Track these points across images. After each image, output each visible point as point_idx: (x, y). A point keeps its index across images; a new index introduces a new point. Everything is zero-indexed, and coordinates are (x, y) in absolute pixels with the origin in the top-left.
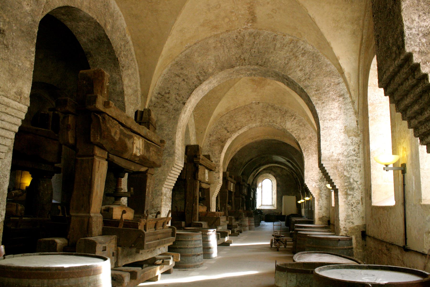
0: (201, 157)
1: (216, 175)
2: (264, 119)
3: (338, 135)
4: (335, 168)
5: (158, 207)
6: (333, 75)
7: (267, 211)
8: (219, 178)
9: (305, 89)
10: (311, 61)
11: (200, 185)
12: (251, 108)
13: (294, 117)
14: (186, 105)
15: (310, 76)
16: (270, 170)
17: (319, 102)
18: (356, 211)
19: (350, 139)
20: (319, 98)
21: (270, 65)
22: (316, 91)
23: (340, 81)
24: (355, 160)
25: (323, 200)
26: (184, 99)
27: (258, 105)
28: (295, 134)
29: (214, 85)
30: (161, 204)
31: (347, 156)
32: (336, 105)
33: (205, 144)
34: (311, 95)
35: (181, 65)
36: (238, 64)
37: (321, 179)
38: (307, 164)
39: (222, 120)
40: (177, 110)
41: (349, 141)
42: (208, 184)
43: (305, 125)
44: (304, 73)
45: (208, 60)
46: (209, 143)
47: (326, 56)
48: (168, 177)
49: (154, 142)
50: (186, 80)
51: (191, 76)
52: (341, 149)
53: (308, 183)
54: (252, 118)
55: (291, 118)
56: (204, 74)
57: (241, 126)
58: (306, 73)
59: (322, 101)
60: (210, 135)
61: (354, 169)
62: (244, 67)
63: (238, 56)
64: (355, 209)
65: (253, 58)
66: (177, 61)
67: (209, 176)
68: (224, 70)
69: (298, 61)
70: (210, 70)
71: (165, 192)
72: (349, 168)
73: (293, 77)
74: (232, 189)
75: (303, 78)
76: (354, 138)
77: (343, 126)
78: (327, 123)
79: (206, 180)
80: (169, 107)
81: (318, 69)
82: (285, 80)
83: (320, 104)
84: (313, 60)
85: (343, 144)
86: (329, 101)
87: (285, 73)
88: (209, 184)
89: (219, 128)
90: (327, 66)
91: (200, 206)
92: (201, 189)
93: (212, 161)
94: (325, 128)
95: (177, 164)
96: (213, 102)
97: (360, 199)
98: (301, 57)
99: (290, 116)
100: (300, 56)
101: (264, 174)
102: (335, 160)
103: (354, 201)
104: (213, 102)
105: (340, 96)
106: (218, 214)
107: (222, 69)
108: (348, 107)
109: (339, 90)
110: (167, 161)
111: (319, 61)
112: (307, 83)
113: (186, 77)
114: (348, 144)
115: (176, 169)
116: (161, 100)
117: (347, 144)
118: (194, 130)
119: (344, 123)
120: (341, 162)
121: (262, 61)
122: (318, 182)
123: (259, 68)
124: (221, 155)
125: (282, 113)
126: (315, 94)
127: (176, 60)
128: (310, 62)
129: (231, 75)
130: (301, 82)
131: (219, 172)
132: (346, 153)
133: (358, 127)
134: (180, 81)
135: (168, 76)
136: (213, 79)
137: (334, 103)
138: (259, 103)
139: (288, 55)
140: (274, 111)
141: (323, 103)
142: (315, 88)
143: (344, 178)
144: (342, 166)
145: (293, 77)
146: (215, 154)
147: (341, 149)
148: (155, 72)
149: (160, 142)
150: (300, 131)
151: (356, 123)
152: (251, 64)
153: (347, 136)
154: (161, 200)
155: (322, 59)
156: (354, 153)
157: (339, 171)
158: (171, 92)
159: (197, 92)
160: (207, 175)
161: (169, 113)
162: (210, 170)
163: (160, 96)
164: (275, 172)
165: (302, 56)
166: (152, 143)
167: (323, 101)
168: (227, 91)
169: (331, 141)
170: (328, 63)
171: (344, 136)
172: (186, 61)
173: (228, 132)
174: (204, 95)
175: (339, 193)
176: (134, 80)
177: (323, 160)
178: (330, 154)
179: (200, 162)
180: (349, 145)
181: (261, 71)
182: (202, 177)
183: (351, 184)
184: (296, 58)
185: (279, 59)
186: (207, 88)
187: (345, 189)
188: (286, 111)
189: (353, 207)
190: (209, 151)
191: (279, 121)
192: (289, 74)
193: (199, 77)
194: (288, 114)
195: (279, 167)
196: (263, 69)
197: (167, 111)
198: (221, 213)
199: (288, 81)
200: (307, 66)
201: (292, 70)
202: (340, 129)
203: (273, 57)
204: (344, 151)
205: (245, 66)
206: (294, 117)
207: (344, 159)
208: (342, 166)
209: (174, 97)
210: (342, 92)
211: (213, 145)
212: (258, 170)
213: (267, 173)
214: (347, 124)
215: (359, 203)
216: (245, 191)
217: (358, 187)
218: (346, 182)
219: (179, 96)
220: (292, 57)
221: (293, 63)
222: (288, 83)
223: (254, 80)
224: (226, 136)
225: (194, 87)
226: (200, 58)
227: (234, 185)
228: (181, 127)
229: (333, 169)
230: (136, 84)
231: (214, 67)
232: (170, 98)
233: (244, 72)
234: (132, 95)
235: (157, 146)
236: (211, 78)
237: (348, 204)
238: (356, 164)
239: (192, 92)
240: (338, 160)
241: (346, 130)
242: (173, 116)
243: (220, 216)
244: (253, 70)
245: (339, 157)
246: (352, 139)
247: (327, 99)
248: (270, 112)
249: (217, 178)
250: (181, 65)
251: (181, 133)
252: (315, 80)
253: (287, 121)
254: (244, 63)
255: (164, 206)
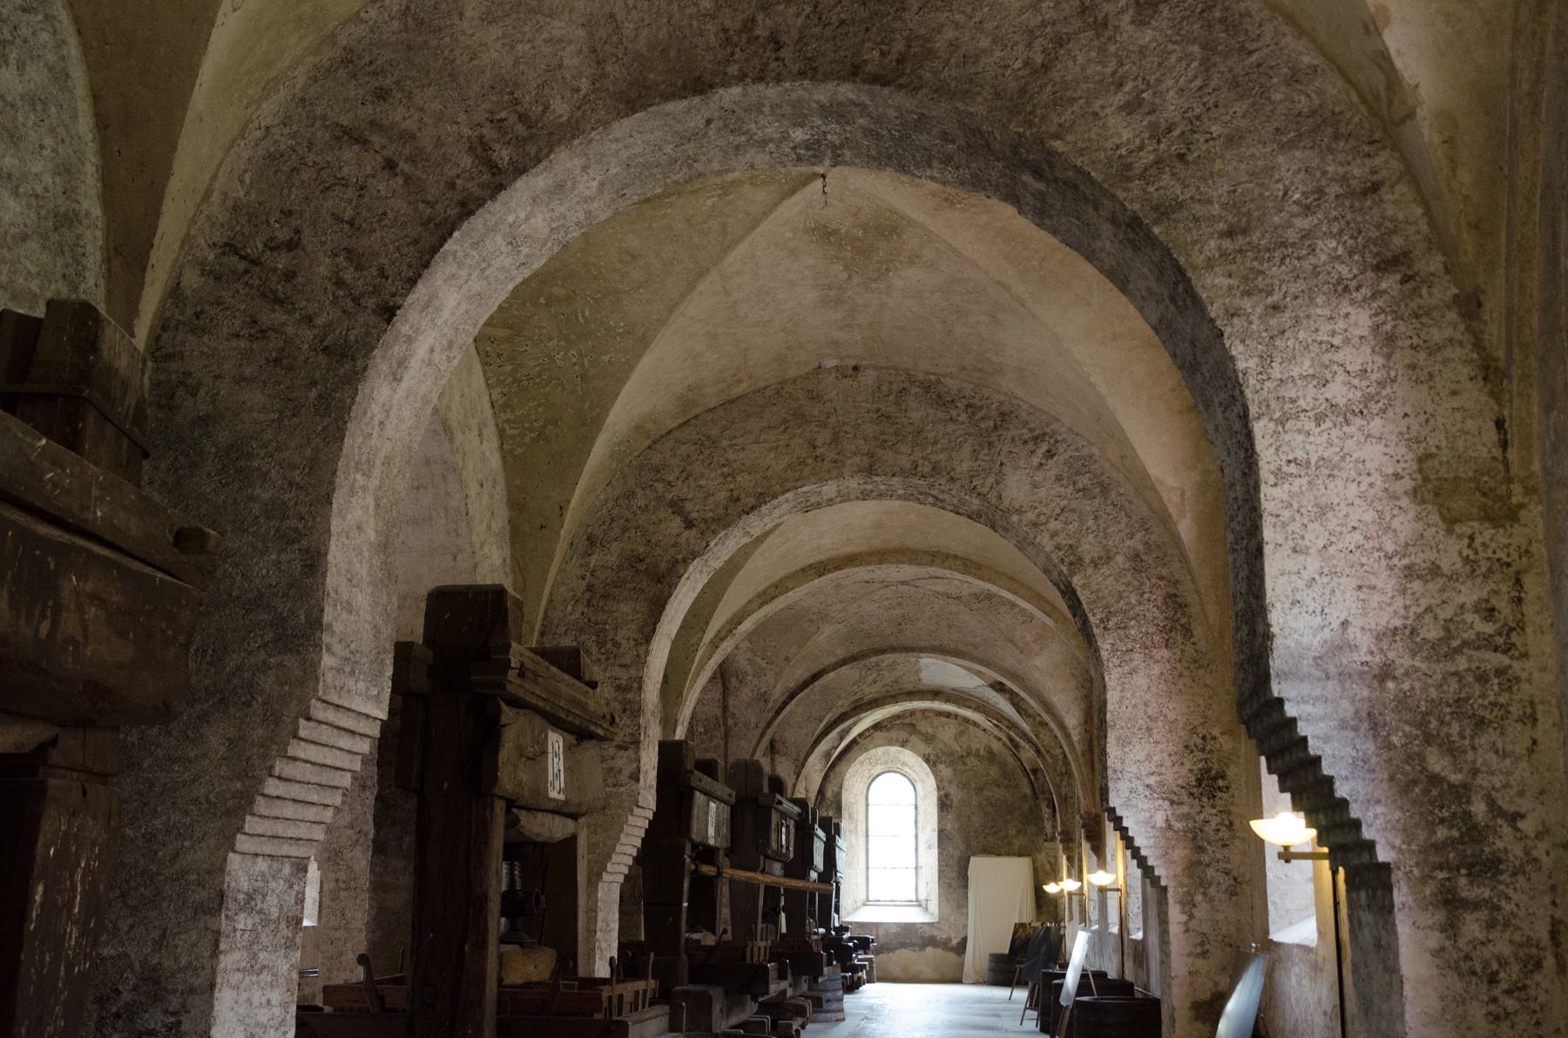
0: (518, 653)
1: (622, 761)
2: (888, 456)
3: (1380, 513)
4: (1365, 726)
5: (192, 990)
6: (1336, 137)
7: (894, 930)
8: (635, 777)
9: (1156, 222)
10: (1196, 48)
11: (513, 823)
12: (815, 397)
13: (1044, 447)
14: (403, 325)
15: (1188, 144)
16: (903, 730)
17: (1247, 304)
18: (1522, 1021)
19: (1460, 537)
20: (1246, 278)
21: (936, 73)
22: (1230, 233)
23: (1385, 173)
24: (1500, 672)
25: (1211, 900)
26: (390, 287)
27: (847, 382)
28: (1054, 535)
29: (588, 213)
30: (214, 972)
31: (1445, 648)
32: (1362, 320)
33: (563, 589)
34: (1199, 259)
35: (375, 73)
36: (733, 70)
37: (1199, 781)
38: (1121, 701)
39: (656, 458)
40: (344, 356)
41: (1450, 555)
42: (560, 810)
43: (1105, 490)
44: (1153, 126)
45: (548, 41)
46: (584, 583)
47: (1291, 20)
48: (272, 788)
49: (108, 537)
50: (404, 166)
51: (439, 143)
52: (1399, 601)
53: (1127, 804)
54: (818, 452)
55: (1032, 452)
56: (520, 129)
57: (761, 494)
58: (1163, 126)
59: (1270, 300)
60: (591, 540)
61: (1491, 735)
62: (772, 92)
63: (733, 22)
64: (1510, 1004)
65: (827, 32)
66: (348, 50)
67: (569, 770)
68: (644, 107)
69: (1112, 48)
70: (561, 108)
71: (245, 885)
72: (1455, 729)
73: (1081, 152)
74: (711, 831)
75: (1147, 158)
76: (1486, 533)
77: (1410, 456)
78: (1300, 438)
79: (553, 794)
80: (290, 330)
81: (1242, 97)
82: (1026, 178)
83: (1254, 318)
84: (1209, 47)
85: (1409, 567)
86: (1311, 299)
87: (1030, 124)
88: (574, 817)
89: (642, 503)
90: (1295, 78)
91: (505, 948)
92: (517, 849)
93: (593, 685)
94: (1292, 469)
95: (334, 698)
96: (605, 358)
97: (1542, 932)
98: (1131, 28)
99: (1026, 442)
100: (1127, 18)
101: (875, 747)
102: (1361, 674)
103: (1506, 950)
104: (605, 358)
105: (1384, 265)
106: (621, 997)
107: (634, 99)
108: (1438, 335)
109: (1378, 227)
110: (267, 682)
111: (1243, 48)
112: (1168, 186)
113: (407, 152)
114: (1446, 570)
115: (325, 734)
116: (239, 286)
117: (1435, 570)
118: (502, 512)
119: (1413, 434)
120: (1406, 686)
121: (883, 54)
122: (1185, 798)
123: (865, 99)
124: (647, 652)
125: (983, 425)
126: (1224, 254)
127: (343, 40)
128: (1189, 57)
129: (690, 148)
130: (1129, 179)
131: (637, 743)
132: (1432, 632)
133: (1506, 462)
134: (369, 170)
135: (293, 136)
136: (578, 162)
137: (1345, 307)
138: (855, 368)
139: (1050, 15)
140: (940, 415)
141: (1276, 308)
142: (1221, 218)
143: (1426, 791)
144: (1408, 717)
145: (1081, 152)
146: (616, 644)
147: (1399, 601)
148: (199, 99)
149: (176, 545)
150: (1082, 521)
151: (1491, 433)
152: (815, 69)
153: (1435, 518)
154: (216, 944)
155: (1267, 38)
156: (1489, 628)
157: (1389, 746)
158: (307, 238)
159: (475, 245)
160: (556, 764)
161: (290, 369)
162: (580, 734)
163: (233, 260)
164: (929, 739)
165: (1140, 22)
166: (82, 542)
167: (1276, 298)
168: (683, 296)
169: (1332, 550)
170: (1306, 60)
171: (1418, 518)
172: (409, 48)
173: (689, 524)
174: (527, 273)
175: (1401, 895)
176: (48, 141)
177: (1285, 675)
178: (1327, 634)
179: (509, 688)
180: (1453, 577)
181: (878, 120)
182: (524, 776)
183: (1474, 833)
184: (1098, 36)
185: (994, 41)
186: (539, 224)
187: (1441, 867)
188: (1003, 414)
189: (1497, 992)
190: (582, 631)
191: (966, 466)
192: (1053, 129)
193: (486, 148)
194: (1014, 432)
195: (948, 715)
196: (890, 103)
197: (277, 361)
198: (640, 985)
199: (1040, 186)
200: (1171, 82)
201: (1076, 107)
202: (1390, 471)
203: (957, 26)
204: (1419, 617)
205: (778, 80)
206: (1044, 447)
207: (1423, 666)
208: (1408, 717)
209: (323, 268)
210: (1398, 241)
211: (605, 597)
212: (847, 731)
213: (891, 743)
214: (1432, 442)
215: (1538, 965)
216: (784, 838)
217: (1527, 852)
218: (1442, 821)
219: (359, 268)
220: (1077, 23)
221: (1080, 62)
222: (1040, 196)
223: (835, 232)
224: (675, 545)
225: (454, 212)
226: (495, 31)
227: (727, 809)
228: (370, 463)
229: (1351, 734)
230: (66, 171)
231: (584, 85)
232: (300, 280)
233: (773, 130)
234: (24, 238)
235: (126, 560)
236: (565, 161)
237: (1464, 966)
238: (1502, 700)
239: (443, 241)
240: (1385, 674)
241: (1426, 479)
242: (313, 393)
243: (634, 1007)
244: (825, 111)
245: (1391, 655)
246: (1472, 538)
247: (1300, 285)
248: (915, 416)
249: (624, 778)
250: (375, 73)
251: (371, 502)
252: (1218, 165)
253: (1006, 469)
254: (773, 65)
255: (236, 978)
